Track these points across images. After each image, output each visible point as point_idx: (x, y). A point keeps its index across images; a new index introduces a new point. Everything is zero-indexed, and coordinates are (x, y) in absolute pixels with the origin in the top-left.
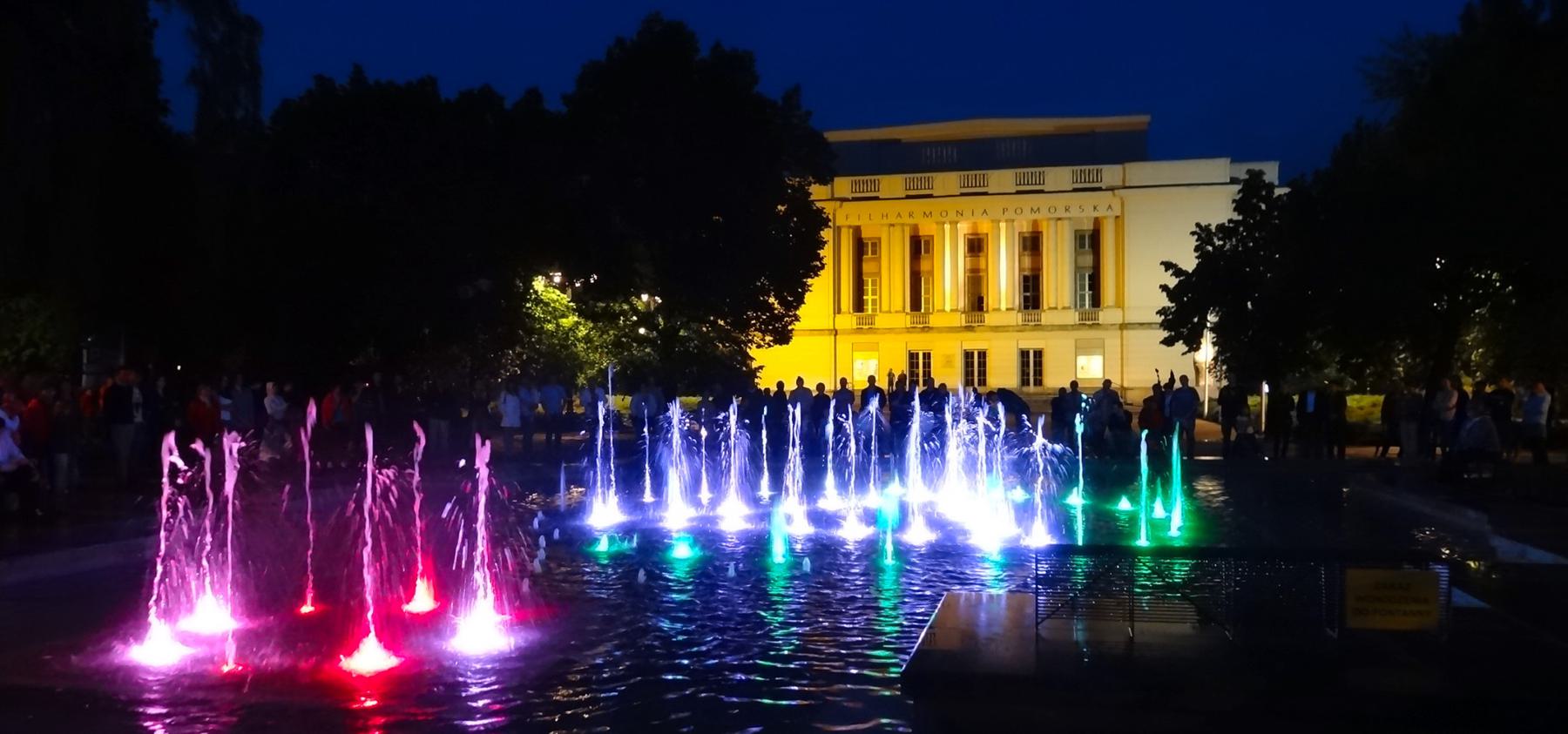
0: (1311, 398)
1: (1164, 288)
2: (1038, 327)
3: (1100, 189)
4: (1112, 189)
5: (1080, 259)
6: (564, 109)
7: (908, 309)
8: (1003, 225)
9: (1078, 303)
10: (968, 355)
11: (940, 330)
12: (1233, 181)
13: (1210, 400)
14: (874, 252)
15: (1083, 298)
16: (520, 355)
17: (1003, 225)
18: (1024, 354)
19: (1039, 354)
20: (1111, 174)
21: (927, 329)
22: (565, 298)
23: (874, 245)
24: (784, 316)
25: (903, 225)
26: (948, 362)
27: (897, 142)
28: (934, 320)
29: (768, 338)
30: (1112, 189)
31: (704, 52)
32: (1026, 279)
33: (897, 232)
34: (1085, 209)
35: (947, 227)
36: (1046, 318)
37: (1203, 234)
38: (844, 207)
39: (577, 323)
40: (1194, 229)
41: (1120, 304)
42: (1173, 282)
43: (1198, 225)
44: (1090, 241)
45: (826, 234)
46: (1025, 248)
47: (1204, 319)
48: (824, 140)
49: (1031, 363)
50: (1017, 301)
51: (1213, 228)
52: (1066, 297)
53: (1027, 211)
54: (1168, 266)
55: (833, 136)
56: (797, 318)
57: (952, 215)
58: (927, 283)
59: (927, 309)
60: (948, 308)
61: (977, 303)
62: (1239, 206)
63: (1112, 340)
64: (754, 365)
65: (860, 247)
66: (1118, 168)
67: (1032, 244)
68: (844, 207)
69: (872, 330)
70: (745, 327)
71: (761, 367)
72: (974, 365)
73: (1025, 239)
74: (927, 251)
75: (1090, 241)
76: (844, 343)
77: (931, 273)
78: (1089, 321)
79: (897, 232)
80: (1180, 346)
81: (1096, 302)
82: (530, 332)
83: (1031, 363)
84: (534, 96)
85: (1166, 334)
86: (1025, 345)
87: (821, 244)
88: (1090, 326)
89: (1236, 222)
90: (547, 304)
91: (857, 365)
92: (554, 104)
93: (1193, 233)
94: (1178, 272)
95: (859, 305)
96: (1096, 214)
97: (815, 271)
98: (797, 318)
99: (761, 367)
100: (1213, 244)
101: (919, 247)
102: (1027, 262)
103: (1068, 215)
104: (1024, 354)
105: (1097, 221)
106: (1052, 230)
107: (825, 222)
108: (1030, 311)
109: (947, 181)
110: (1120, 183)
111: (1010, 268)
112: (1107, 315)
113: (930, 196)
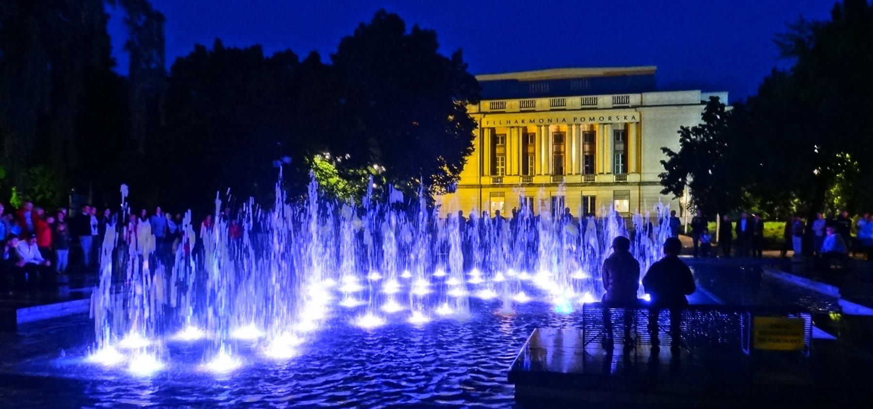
0: (744, 223)
1: (663, 162)
2: (593, 184)
3: (628, 107)
4: (635, 107)
5: (617, 146)
6: (331, 63)
7: (521, 174)
8: (574, 127)
9: (615, 171)
11: (540, 185)
12: (703, 103)
13: (688, 224)
14: (502, 142)
15: (618, 167)
17: (574, 127)
18: (585, 199)
19: (593, 199)
20: (634, 98)
21: (531, 185)
22: (332, 167)
23: (502, 138)
25: (518, 127)
26: (543, 204)
28: (535, 180)
29: (443, 189)
30: (635, 107)
31: (409, 31)
32: (586, 157)
33: (515, 131)
34: (621, 117)
35: (543, 128)
36: (598, 179)
37: (685, 132)
38: (485, 116)
39: (338, 181)
40: (680, 129)
41: (639, 171)
42: (667, 159)
45: (476, 132)
47: (684, 179)
49: (589, 204)
52: (608, 167)
53: (587, 120)
54: (665, 150)
55: (479, 78)
56: (459, 179)
57: (546, 122)
60: (543, 173)
61: (559, 171)
62: (705, 117)
63: (634, 192)
65: (495, 139)
68: (485, 116)
70: (428, 182)
75: (621, 136)
76: (486, 193)
77: (534, 154)
78: (621, 180)
80: (671, 195)
81: (625, 169)
83: (589, 204)
84: (314, 56)
85: (663, 188)
86: (585, 193)
87: (473, 137)
88: (623, 184)
89: (703, 126)
90: (322, 171)
91: (493, 204)
93: (679, 132)
94: (670, 153)
95: (494, 171)
96: (626, 121)
97: (469, 153)
98: (459, 179)
100: (690, 138)
101: (527, 139)
102: (587, 147)
104: (585, 199)
106: (601, 130)
109: (543, 103)
111: (578, 151)
112: (632, 178)
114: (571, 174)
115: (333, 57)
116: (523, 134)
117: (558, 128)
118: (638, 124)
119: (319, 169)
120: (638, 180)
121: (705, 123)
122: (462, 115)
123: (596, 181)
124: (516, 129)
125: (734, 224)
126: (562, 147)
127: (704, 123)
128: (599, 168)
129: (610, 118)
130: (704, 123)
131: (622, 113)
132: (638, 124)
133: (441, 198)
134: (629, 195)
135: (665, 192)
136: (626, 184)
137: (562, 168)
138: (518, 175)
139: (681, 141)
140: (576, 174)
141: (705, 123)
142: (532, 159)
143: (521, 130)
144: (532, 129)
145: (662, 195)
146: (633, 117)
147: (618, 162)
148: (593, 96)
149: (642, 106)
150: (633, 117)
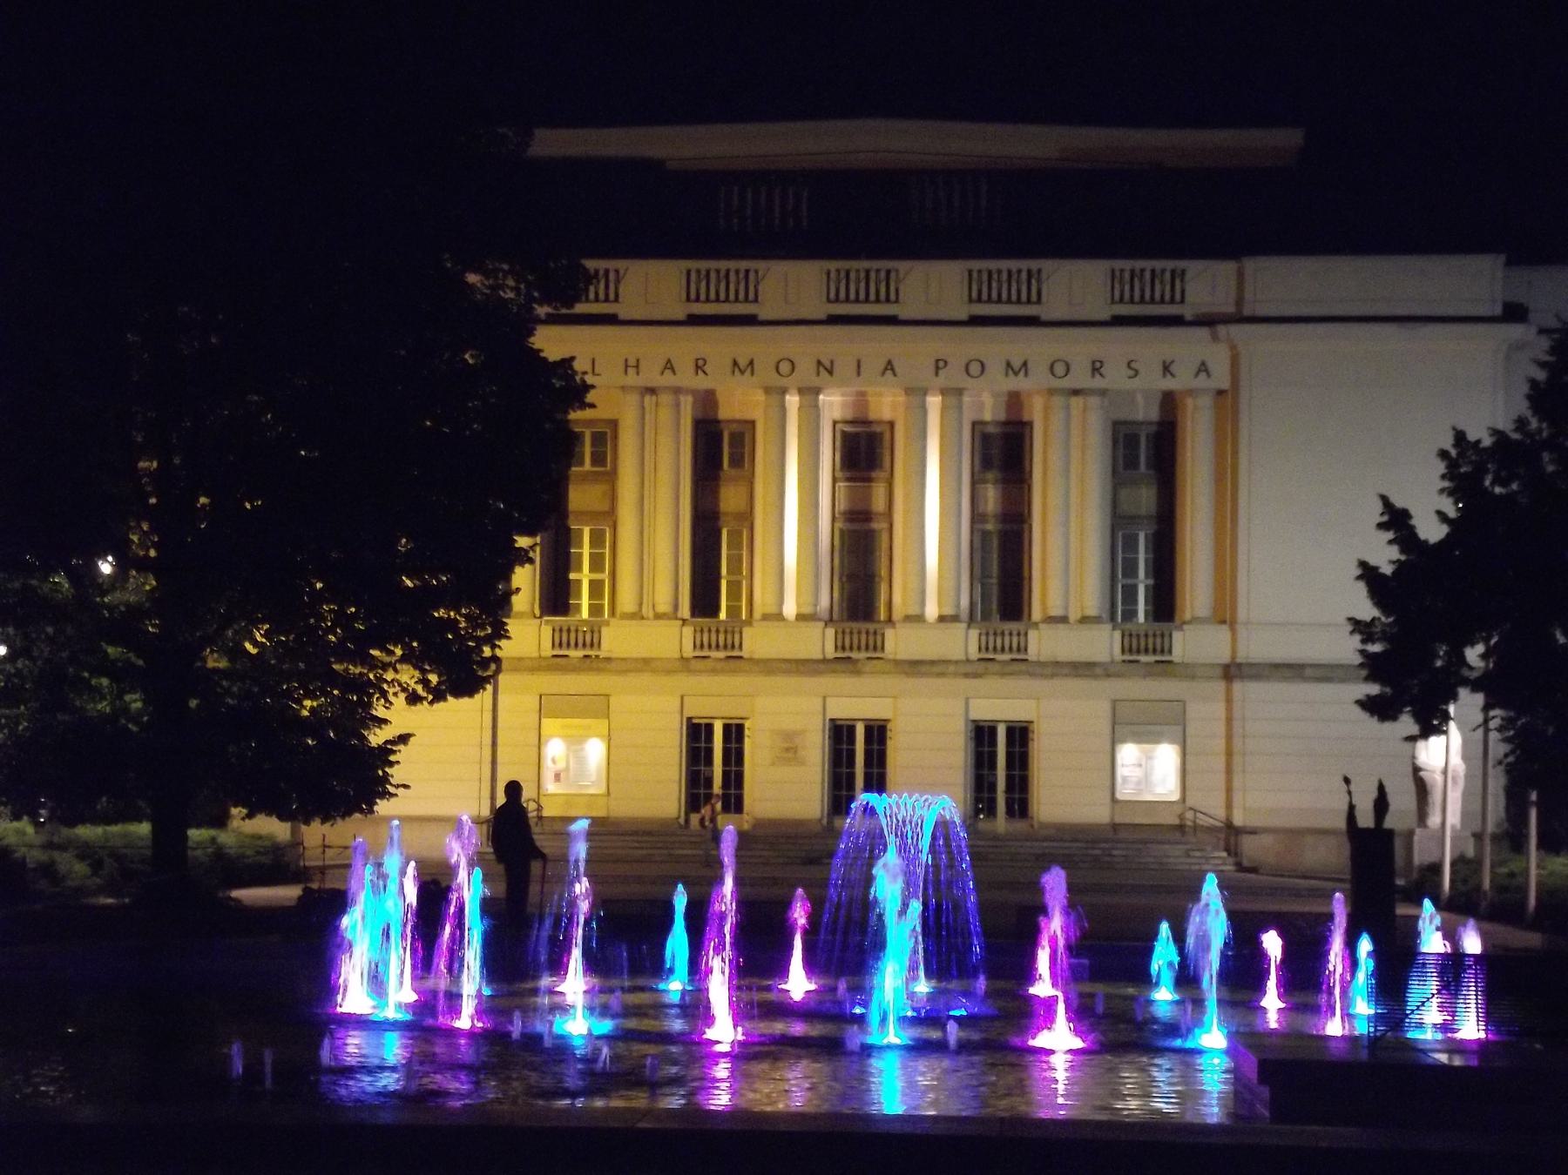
2: (1020, 664)
5: (1124, 493)
7: (685, 611)
8: (934, 402)
9: (1118, 608)
11: (770, 666)
12: (1514, 313)
14: (598, 459)
17: (934, 402)
18: (982, 734)
19: (1020, 735)
20: (1208, 284)
21: (735, 660)
23: (599, 439)
25: (677, 391)
26: (789, 750)
28: (756, 642)
30: (1208, 321)
34: (1141, 367)
35: (793, 401)
36: (1042, 643)
41: (1224, 614)
49: (1000, 762)
52: (1091, 596)
53: (995, 369)
58: (735, 544)
60: (790, 609)
67: (1003, 454)
72: (858, 757)
73: (986, 438)
74: (737, 461)
77: (747, 517)
81: (1165, 605)
83: (1000, 762)
86: (985, 710)
91: (555, 749)
95: (556, 598)
96: (1169, 384)
102: (992, 497)
103: (1098, 382)
104: (982, 734)
105: (1169, 402)
109: (793, 283)
110: (1231, 309)
112: (1195, 642)
113: (750, 320)
117: (861, 400)
118: (1227, 401)
120: (1225, 658)
123: (1033, 652)
124: (666, 399)
129: (1096, 368)
131: (1150, 346)
136: (1166, 668)
138: (674, 614)
142: (735, 544)
143: (687, 403)
144: (740, 401)
146: (1203, 368)
147: (1130, 569)
148: (1024, 264)
150: (1203, 368)
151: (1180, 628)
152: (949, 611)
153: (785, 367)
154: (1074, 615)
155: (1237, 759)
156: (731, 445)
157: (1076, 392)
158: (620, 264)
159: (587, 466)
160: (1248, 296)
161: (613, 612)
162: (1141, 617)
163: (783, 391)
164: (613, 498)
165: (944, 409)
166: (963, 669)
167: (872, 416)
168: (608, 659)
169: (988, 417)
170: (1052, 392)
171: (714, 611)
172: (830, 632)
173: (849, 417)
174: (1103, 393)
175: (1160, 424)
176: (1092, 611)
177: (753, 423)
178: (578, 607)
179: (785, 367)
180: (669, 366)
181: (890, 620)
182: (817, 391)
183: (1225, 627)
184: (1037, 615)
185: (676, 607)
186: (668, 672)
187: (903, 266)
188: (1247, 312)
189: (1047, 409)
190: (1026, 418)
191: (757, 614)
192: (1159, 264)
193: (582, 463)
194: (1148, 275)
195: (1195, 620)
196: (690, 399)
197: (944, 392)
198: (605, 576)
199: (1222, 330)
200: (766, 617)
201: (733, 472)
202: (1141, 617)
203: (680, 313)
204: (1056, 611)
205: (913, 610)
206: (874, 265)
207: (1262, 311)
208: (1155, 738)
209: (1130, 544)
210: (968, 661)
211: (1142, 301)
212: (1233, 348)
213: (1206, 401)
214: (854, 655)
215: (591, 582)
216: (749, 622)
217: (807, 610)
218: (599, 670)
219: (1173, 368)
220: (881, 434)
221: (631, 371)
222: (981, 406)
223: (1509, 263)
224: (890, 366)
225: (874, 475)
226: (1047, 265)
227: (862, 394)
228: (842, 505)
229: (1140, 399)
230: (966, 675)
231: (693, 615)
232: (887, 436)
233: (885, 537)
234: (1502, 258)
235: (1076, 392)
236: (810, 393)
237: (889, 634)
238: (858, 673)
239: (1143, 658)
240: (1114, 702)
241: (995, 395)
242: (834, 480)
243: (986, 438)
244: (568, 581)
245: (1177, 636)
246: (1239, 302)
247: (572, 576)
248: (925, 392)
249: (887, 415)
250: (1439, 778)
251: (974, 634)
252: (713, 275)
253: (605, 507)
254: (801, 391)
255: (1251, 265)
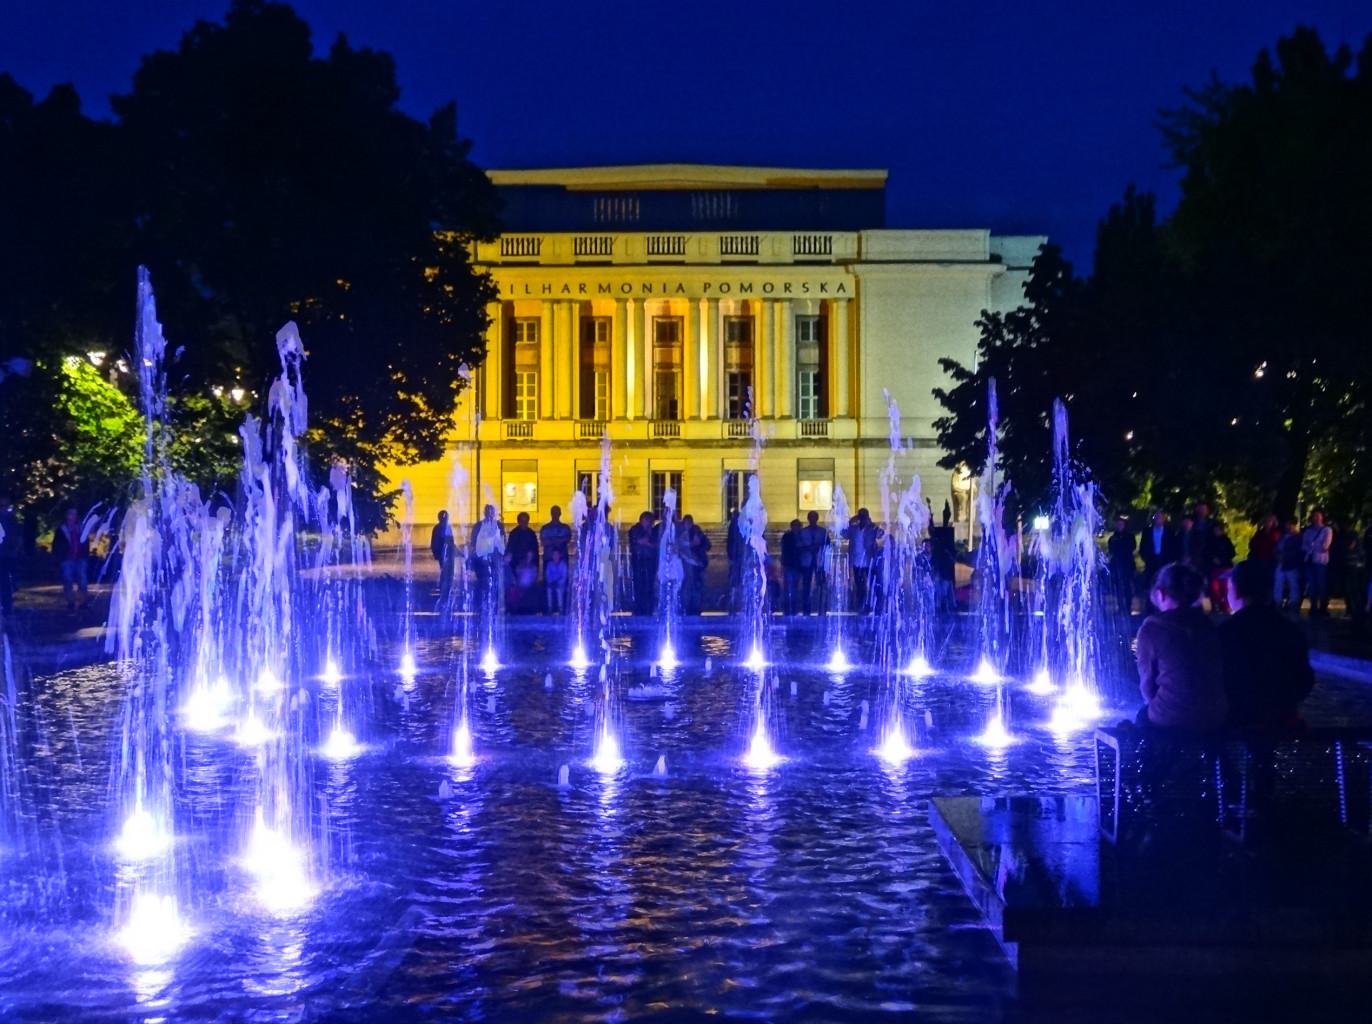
0: (1158, 535)
1: (938, 393)
2: (748, 443)
3: (828, 263)
4: (844, 263)
5: (803, 353)
6: (115, 119)
7: (577, 415)
8: (704, 306)
9: (799, 412)
10: (657, 479)
12: (995, 259)
13: (974, 538)
14: (531, 337)
15: (806, 403)
16: (53, 471)
17: (704, 306)
20: (843, 243)
22: (112, 392)
23: (531, 327)
24: (435, 423)
25: (570, 301)
26: (631, 487)
27: (558, 190)
29: (413, 451)
30: (844, 263)
31: (321, 49)
32: (733, 377)
33: (562, 312)
34: (810, 286)
35: (631, 306)
36: (762, 431)
37: (991, 325)
39: (130, 426)
40: (979, 317)
41: (854, 414)
42: (949, 383)
43: (984, 313)
44: (815, 329)
45: (493, 311)
46: (731, 338)
48: (488, 181)
50: (723, 406)
51: (1002, 318)
52: (785, 405)
53: (735, 288)
54: (948, 364)
55: (500, 177)
56: (451, 424)
57: (637, 290)
58: (603, 379)
59: (603, 415)
60: (631, 415)
61: (668, 409)
62: (1031, 291)
63: (845, 460)
64: (385, 489)
66: (854, 235)
67: (741, 331)
69: (525, 444)
70: (373, 433)
71: (400, 492)
73: (731, 325)
74: (603, 337)
75: (815, 329)
76: (491, 460)
77: (608, 367)
79: (562, 312)
81: (823, 409)
82: (74, 437)
84: (65, 96)
85: (943, 453)
86: (733, 464)
87: (484, 324)
90: (85, 398)
91: (508, 489)
92: (96, 110)
93: (978, 323)
94: (960, 373)
95: (510, 409)
96: (824, 295)
98: (451, 424)
99: (400, 492)
100: (1002, 338)
101: (591, 331)
102: (735, 356)
103: (787, 295)
105: (824, 305)
107: (492, 294)
108: (739, 420)
109: (631, 245)
110: (855, 256)
111: (714, 363)
112: (839, 429)
113: (608, 264)
114: (695, 418)
115: (117, 103)
116: (582, 319)
117: (667, 308)
118: (853, 303)
119: (77, 393)
120: (855, 436)
121: (1033, 306)
122: (457, 265)
124: (565, 305)
125: (1138, 538)
126: (676, 353)
127: (1029, 305)
128: (762, 402)
129: (787, 288)
130: (1029, 305)
132: (853, 303)
133: (397, 473)
134: (833, 469)
135: (947, 463)
136: (825, 442)
137: (673, 405)
139: (980, 345)
140: (710, 418)
141: (1033, 306)
142: (603, 379)
143: (576, 307)
144: (604, 306)
145: (941, 470)
146: (841, 287)
147: (805, 391)
149: (859, 261)
150: (841, 287)
151: (831, 421)
152: (713, 414)
153: (627, 288)
154: (777, 416)
155: (861, 489)
156: (600, 329)
157: (776, 300)
158: (540, 236)
159: (525, 341)
160: (864, 250)
161: (539, 418)
162: (811, 416)
163: (626, 300)
164: (538, 357)
165: (709, 308)
166: (721, 444)
167: (673, 313)
168: (537, 442)
169: (732, 312)
170: (765, 300)
171: (592, 414)
172: (652, 426)
173: (660, 313)
174: (790, 300)
175: (820, 316)
176: (787, 413)
177: (610, 318)
178: (521, 415)
179: (627, 288)
180: (566, 288)
181: (683, 420)
182: (644, 300)
183: (854, 422)
184: (759, 416)
185: (571, 413)
186: (568, 447)
187: (687, 235)
188: (863, 257)
189: (762, 308)
190: (752, 313)
191: (614, 417)
192: (818, 234)
193: (522, 339)
194: (812, 240)
195: (839, 417)
196: (578, 306)
197: (709, 300)
198: (535, 398)
199: (850, 268)
200: (618, 418)
201: (602, 343)
202: (811, 416)
203: (572, 259)
204: (768, 413)
205: (694, 414)
206: (672, 235)
207: (870, 257)
208: (820, 478)
209: (805, 378)
210: (723, 440)
211: (810, 252)
212: (856, 277)
213: (843, 304)
214: (664, 437)
215: (528, 401)
216: (609, 421)
217: (640, 414)
218: (532, 447)
219: (826, 287)
220: (677, 324)
221: (547, 291)
222: (728, 308)
223: (992, 235)
224: (680, 287)
225: (674, 344)
226: (761, 235)
227: (667, 302)
228: (658, 359)
229: (810, 304)
230: (723, 447)
231: (582, 416)
232: (680, 324)
233: (679, 376)
234: (988, 232)
235: (776, 300)
236: (639, 301)
237: (682, 426)
238: (667, 447)
239: (813, 437)
240: (798, 460)
241: (736, 302)
242: (653, 347)
243: (731, 325)
244: (516, 402)
245: (829, 425)
246: (859, 253)
247: (518, 398)
248: (699, 300)
249: (680, 314)
250: (965, 496)
251: (726, 425)
252: (588, 241)
253: (535, 362)
254: (635, 300)
255: (865, 233)
